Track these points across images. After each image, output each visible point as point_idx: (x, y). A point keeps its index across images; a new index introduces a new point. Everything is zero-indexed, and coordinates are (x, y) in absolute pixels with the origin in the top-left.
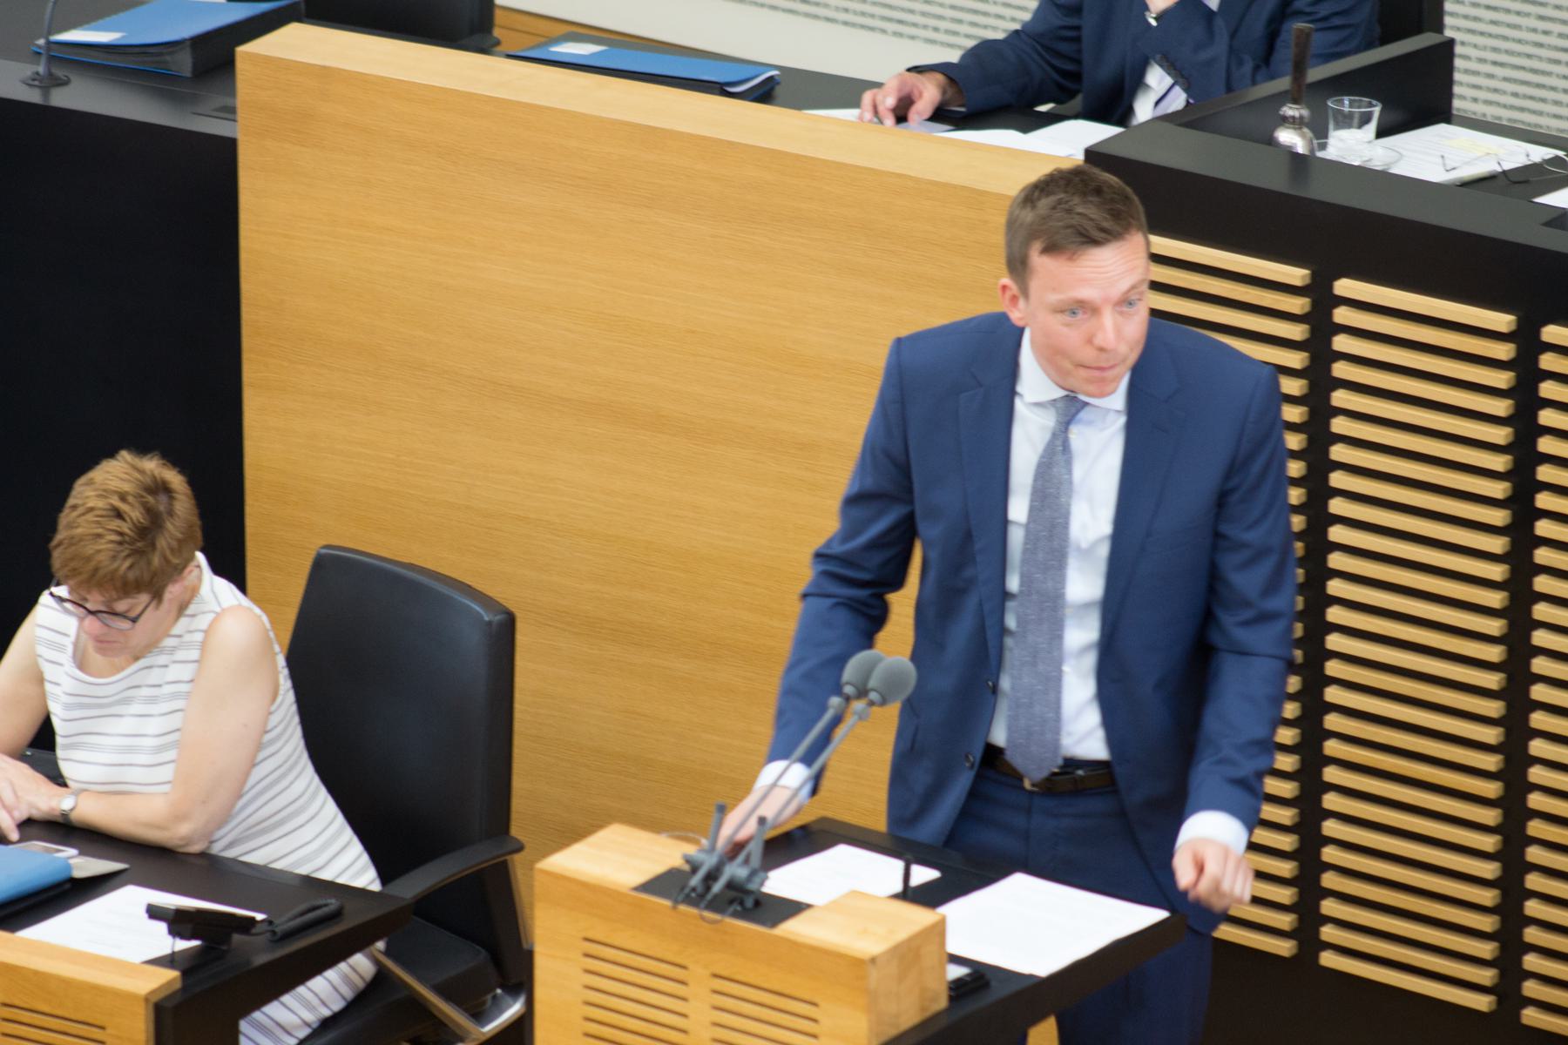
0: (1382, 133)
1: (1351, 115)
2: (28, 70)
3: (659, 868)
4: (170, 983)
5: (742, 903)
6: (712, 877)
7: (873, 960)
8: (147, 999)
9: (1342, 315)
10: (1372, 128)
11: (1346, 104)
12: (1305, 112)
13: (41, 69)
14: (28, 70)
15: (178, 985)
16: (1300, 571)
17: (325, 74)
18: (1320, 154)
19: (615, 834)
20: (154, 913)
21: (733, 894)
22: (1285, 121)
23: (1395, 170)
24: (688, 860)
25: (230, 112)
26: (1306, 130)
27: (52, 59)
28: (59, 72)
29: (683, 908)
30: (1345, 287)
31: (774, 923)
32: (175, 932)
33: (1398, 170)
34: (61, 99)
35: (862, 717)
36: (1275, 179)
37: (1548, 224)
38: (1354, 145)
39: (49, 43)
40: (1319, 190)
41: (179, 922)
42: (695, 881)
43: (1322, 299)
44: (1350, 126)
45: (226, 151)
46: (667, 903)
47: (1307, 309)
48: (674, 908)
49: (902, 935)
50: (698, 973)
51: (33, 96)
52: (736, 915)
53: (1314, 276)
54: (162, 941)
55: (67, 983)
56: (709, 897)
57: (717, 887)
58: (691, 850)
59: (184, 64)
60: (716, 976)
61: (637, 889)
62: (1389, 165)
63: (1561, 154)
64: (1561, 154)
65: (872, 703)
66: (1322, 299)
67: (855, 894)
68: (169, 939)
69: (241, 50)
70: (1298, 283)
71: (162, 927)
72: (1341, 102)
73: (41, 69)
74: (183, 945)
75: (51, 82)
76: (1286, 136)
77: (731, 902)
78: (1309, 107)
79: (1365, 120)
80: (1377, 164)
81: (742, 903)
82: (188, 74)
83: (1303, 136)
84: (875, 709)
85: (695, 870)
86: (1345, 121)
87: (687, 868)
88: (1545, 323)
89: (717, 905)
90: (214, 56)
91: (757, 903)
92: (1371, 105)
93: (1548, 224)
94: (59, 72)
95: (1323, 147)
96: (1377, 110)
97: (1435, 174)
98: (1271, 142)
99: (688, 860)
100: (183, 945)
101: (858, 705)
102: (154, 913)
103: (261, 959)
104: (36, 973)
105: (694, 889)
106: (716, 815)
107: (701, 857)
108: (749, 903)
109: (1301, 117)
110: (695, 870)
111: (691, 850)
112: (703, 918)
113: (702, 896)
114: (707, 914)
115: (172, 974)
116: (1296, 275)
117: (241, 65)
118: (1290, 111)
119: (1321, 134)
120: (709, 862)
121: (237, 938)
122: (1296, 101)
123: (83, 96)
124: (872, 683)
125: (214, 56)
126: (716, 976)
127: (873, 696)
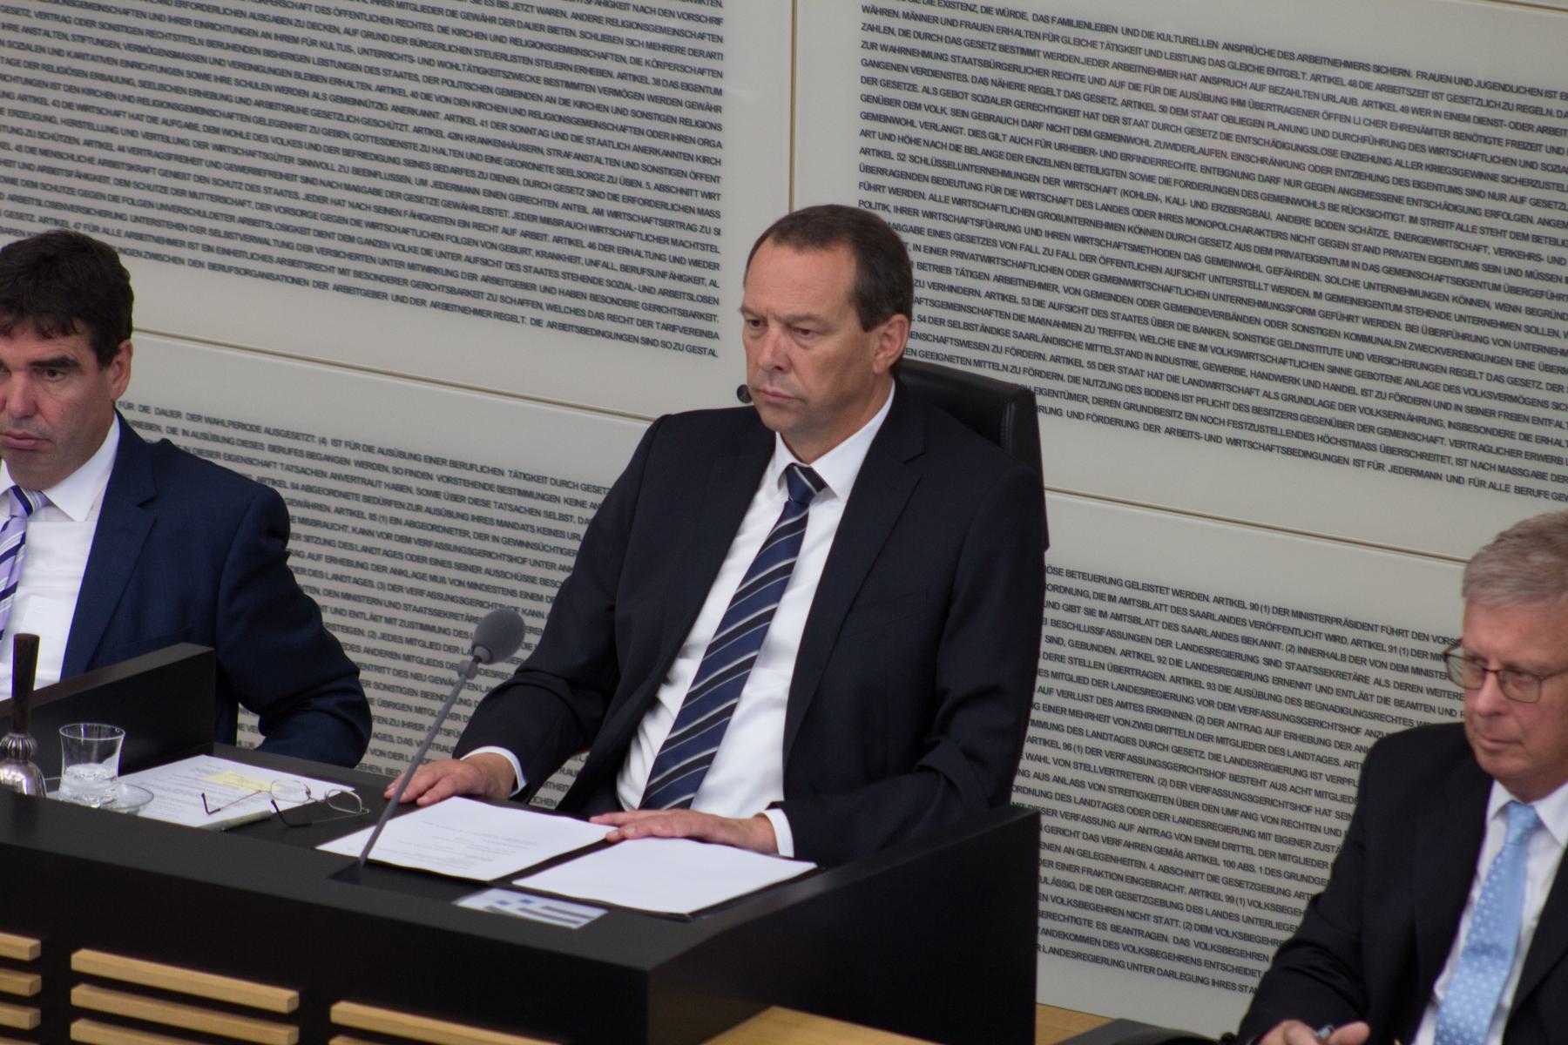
0: (124, 769)
1: (88, 746)
18: (50, 795)
23: (145, 813)
33: (150, 812)
37: (337, 876)
38: (91, 783)
40: (51, 840)
44: (87, 760)
62: (137, 807)
63: (349, 790)
64: (349, 790)
70: (26, 956)
79: (104, 754)
80: (122, 806)
88: (336, 1000)
92: (113, 733)
93: (337, 876)
95: (55, 786)
96: (121, 739)
97: (195, 818)
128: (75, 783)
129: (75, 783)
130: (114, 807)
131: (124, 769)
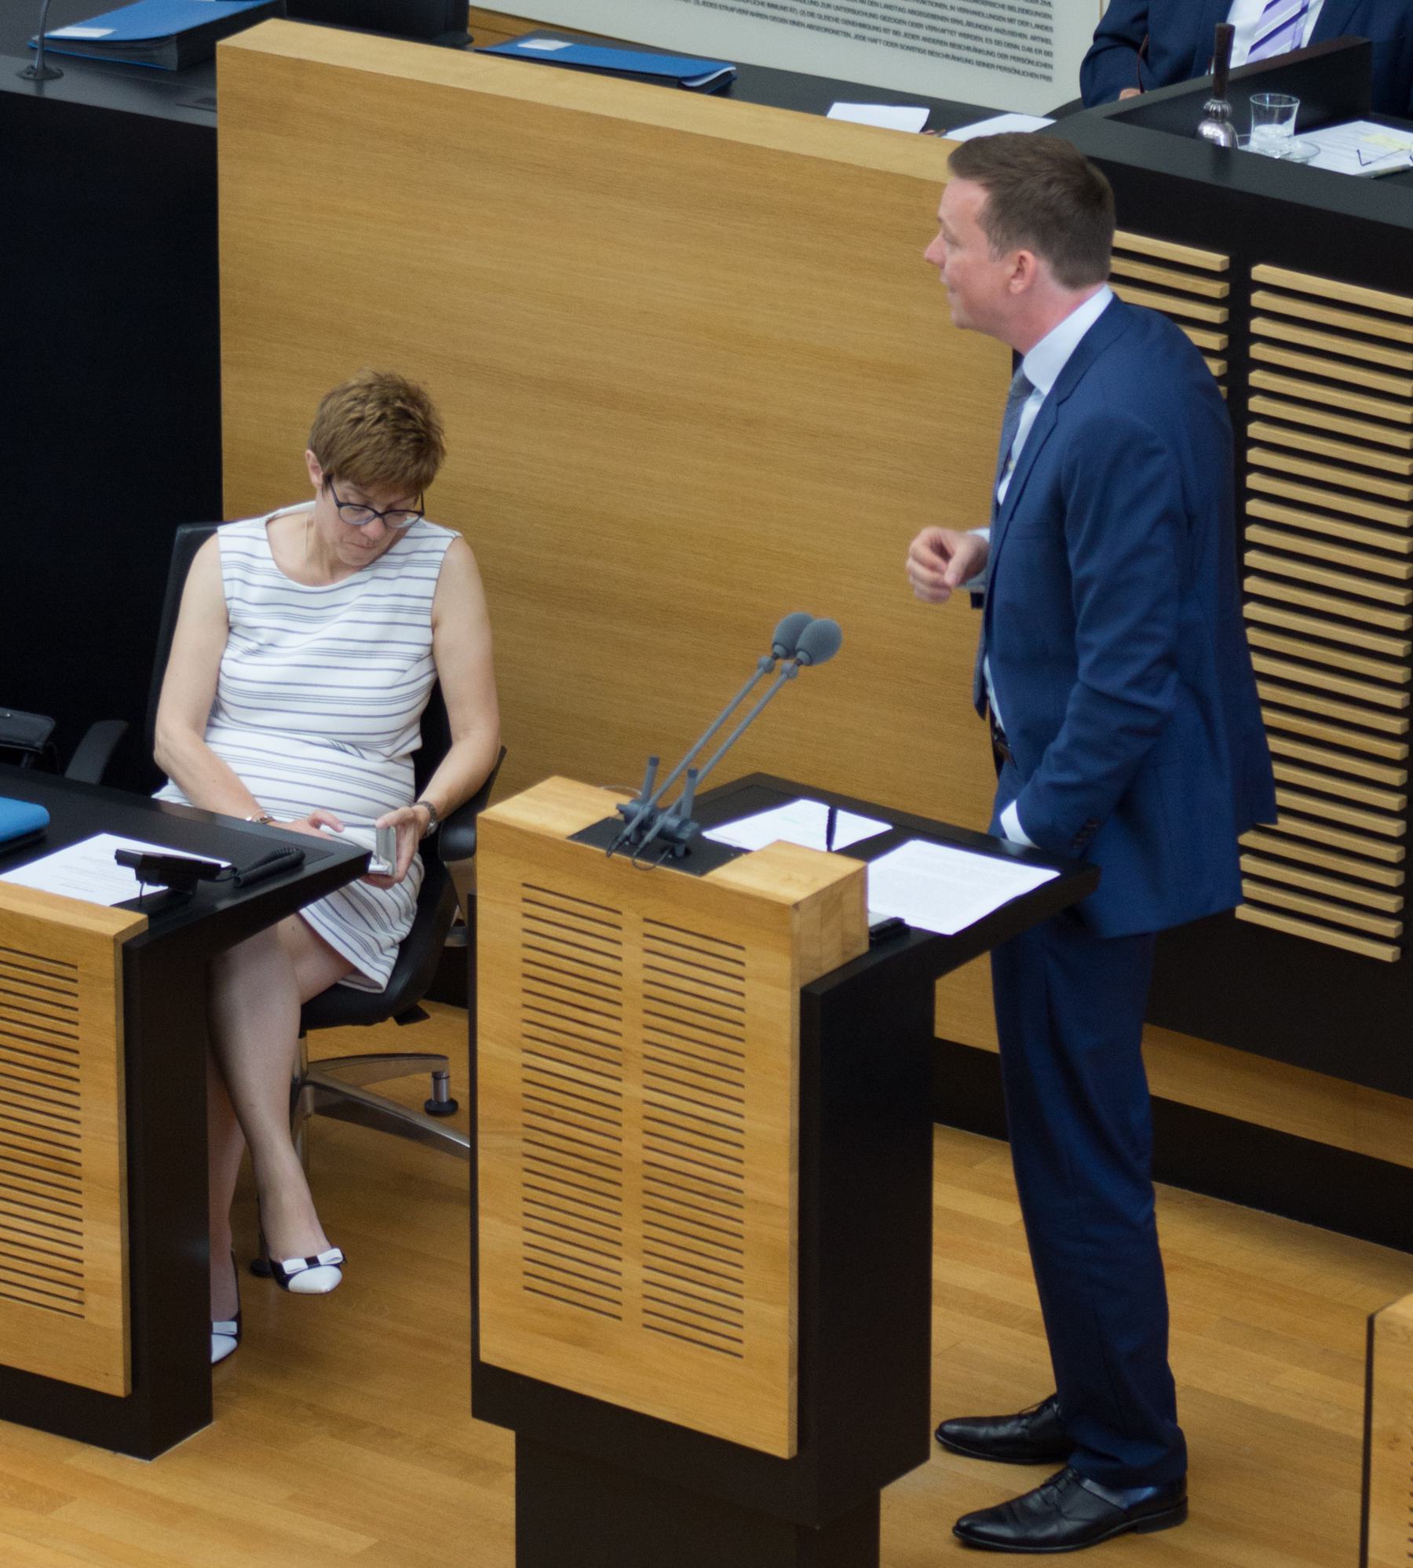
0: (1300, 129)
1: (1271, 111)
2: (22, 64)
3: (594, 818)
4: (137, 925)
5: (673, 852)
6: (644, 826)
7: (796, 906)
8: (115, 939)
9: (1258, 299)
10: (1291, 124)
11: (1267, 101)
12: (1227, 107)
13: (36, 63)
14: (22, 64)
15: (146, 928)
16: (1223, 389)
17: (299, 66)
19: (554, 785)
20: (122, 858)
21: (662, 843)
22: (1208, 116)
24: (621, 809)
25: (210, 103)
26: (1228, 124)
27: (46, 54)
28: (53, 66)
29: (615, 855)
30: (1262, 272)
31: (703, 873)
32: (142, 877)
33: (1318, 162)
34: (55, 91)
35: (790, 675)
36: (1199, 171)
38: (1273, 139)
39: (43, 39)
40: (1240, 181)
41: (146, 868)
42: (629, 830)
43: (1240, 284)
45: (207, 138)
46: (602, 851)
47: (1226, 293)
48: (609, 856)
49: (824, 882)
50: (630, 919)
51: (27, 88)
52: (667, 863)
53: (1232, 262)
54: (129, 885)
55: (41, 925)
56: (641, 846)
57: (649, 836)
58: (625, 800)
59: (170, 58)
60: (647, 920)
61: (573, 837)
62: (1308, 158)
65: (799, 663)
66: (1240, 284)
67: (779, 843)
68: (138, 884)
69: (222, 43)
70: (1217, 268)
71: (130, 872)
72: (1263, 99)
73: (36, 63)
74: (150, 890)
75: (44, 75)
76: (1209, 130)
77: (662, 852)
78: (1231, 102)
79: (1284, 117)
80: (1297, 157)
81: (673, 852)
82: (173, 66)
83: (1225, 130)
84: (802, 669)
85: (628, 819)
86: (1266, 117)
87: (621, 817)
89: (648, 853)
90: (196, 51)
91: (687, 852)
92: (1290, 101)
94: (53, 66)
95: (1246, 140)
96: (1296, 106)
97: (1350, 167)
98: (1196, 134)
99: (621, 809)
100: (150, 890)
101: (788, 664)
102: (122, 858)
103: (224, 905)
104: (12, 914)
105: (627, 838)
106: (649, 768)
107: (635, 807)
108: (680, 851)
109: (1223, 112)
110: (628, 819)
111: (625, 800)
112: (635, 865)
113: (635, 845)
114: (638, 861)
115: (139, 917)
116: (1215, 260)
117: (220, 58)
118: (1213, 105)
119: (1241, 127)
120: (643, 811)
121: (201, 883)
122: (1219, 96)
123: (74, 88)
124: (799, 644)
125: (196, 51)
126: (647, 920)
127: (801, 655)
128: (1262, 139)
129: (1262, 139)
130: (1291, 158)
131: (1300, 129)
